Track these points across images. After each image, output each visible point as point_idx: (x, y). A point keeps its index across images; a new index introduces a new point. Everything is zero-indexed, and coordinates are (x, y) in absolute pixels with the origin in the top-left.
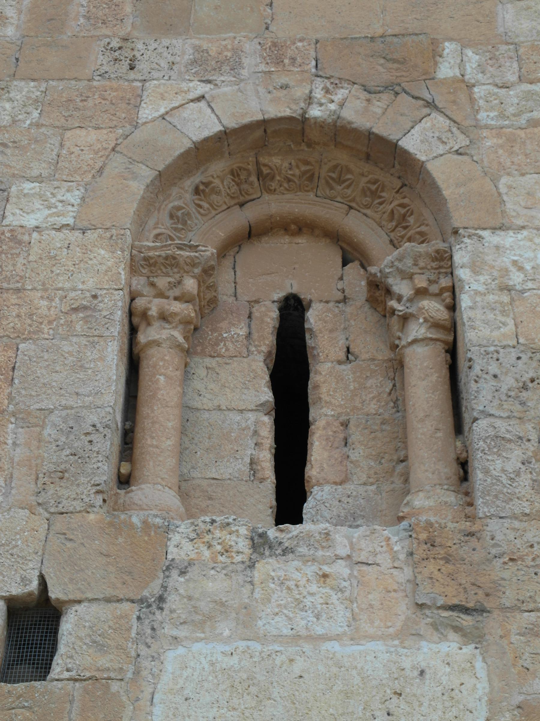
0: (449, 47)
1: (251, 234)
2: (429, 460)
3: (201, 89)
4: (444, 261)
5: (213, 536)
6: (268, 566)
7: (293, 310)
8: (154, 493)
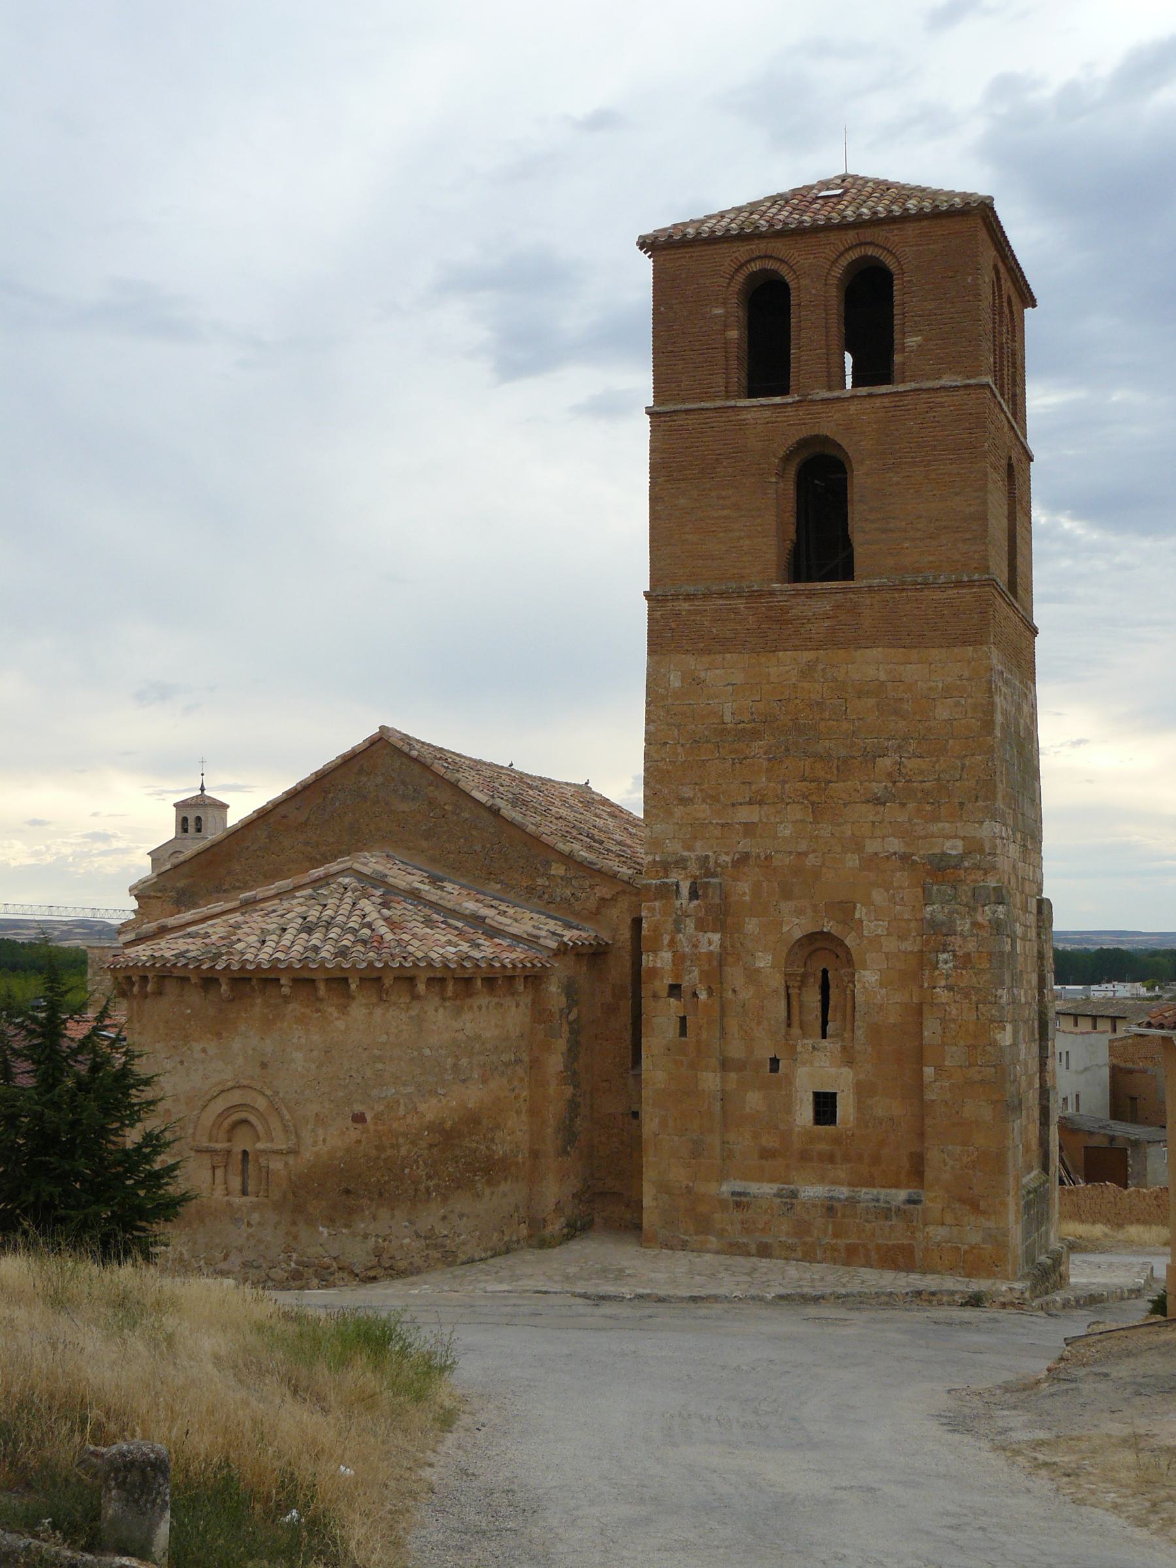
0: (859, 905)
1: (815, 951)
2: (849, 1027)
3: (797, 921)
4: (854, 975)
5: (803, 1045)
6: (816, 1053)
7: (825, 972)
8: (796, 1031)
